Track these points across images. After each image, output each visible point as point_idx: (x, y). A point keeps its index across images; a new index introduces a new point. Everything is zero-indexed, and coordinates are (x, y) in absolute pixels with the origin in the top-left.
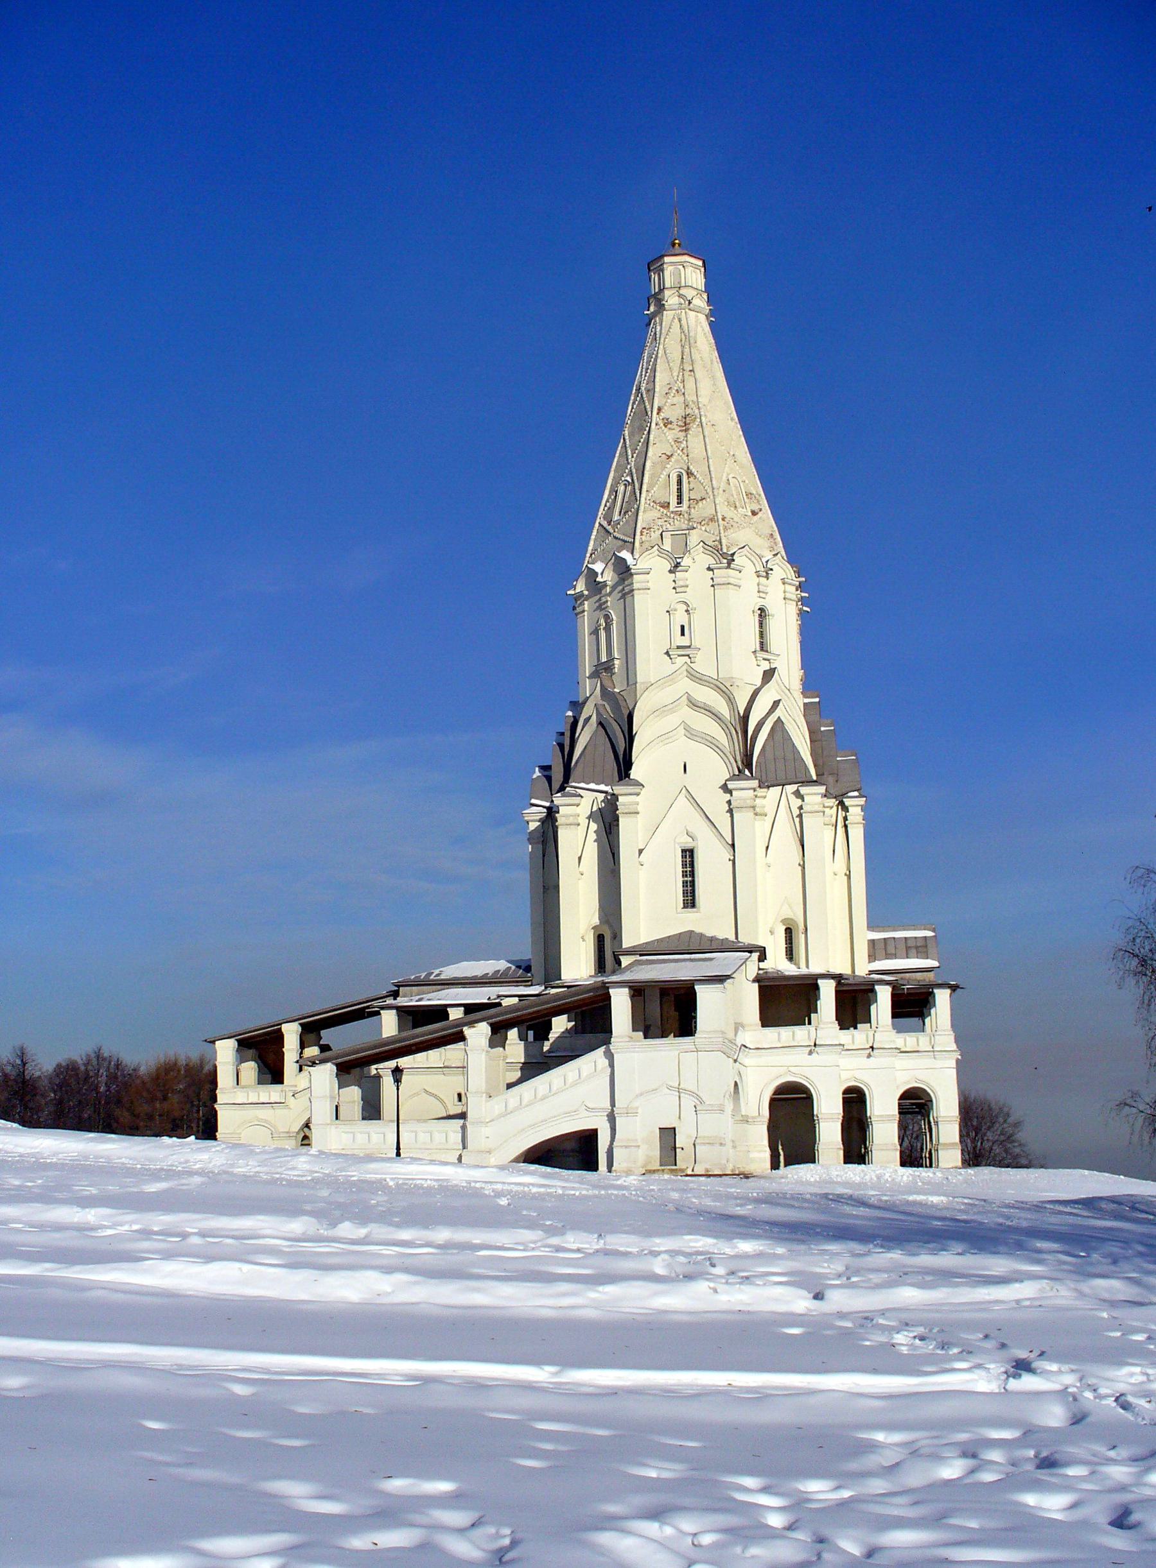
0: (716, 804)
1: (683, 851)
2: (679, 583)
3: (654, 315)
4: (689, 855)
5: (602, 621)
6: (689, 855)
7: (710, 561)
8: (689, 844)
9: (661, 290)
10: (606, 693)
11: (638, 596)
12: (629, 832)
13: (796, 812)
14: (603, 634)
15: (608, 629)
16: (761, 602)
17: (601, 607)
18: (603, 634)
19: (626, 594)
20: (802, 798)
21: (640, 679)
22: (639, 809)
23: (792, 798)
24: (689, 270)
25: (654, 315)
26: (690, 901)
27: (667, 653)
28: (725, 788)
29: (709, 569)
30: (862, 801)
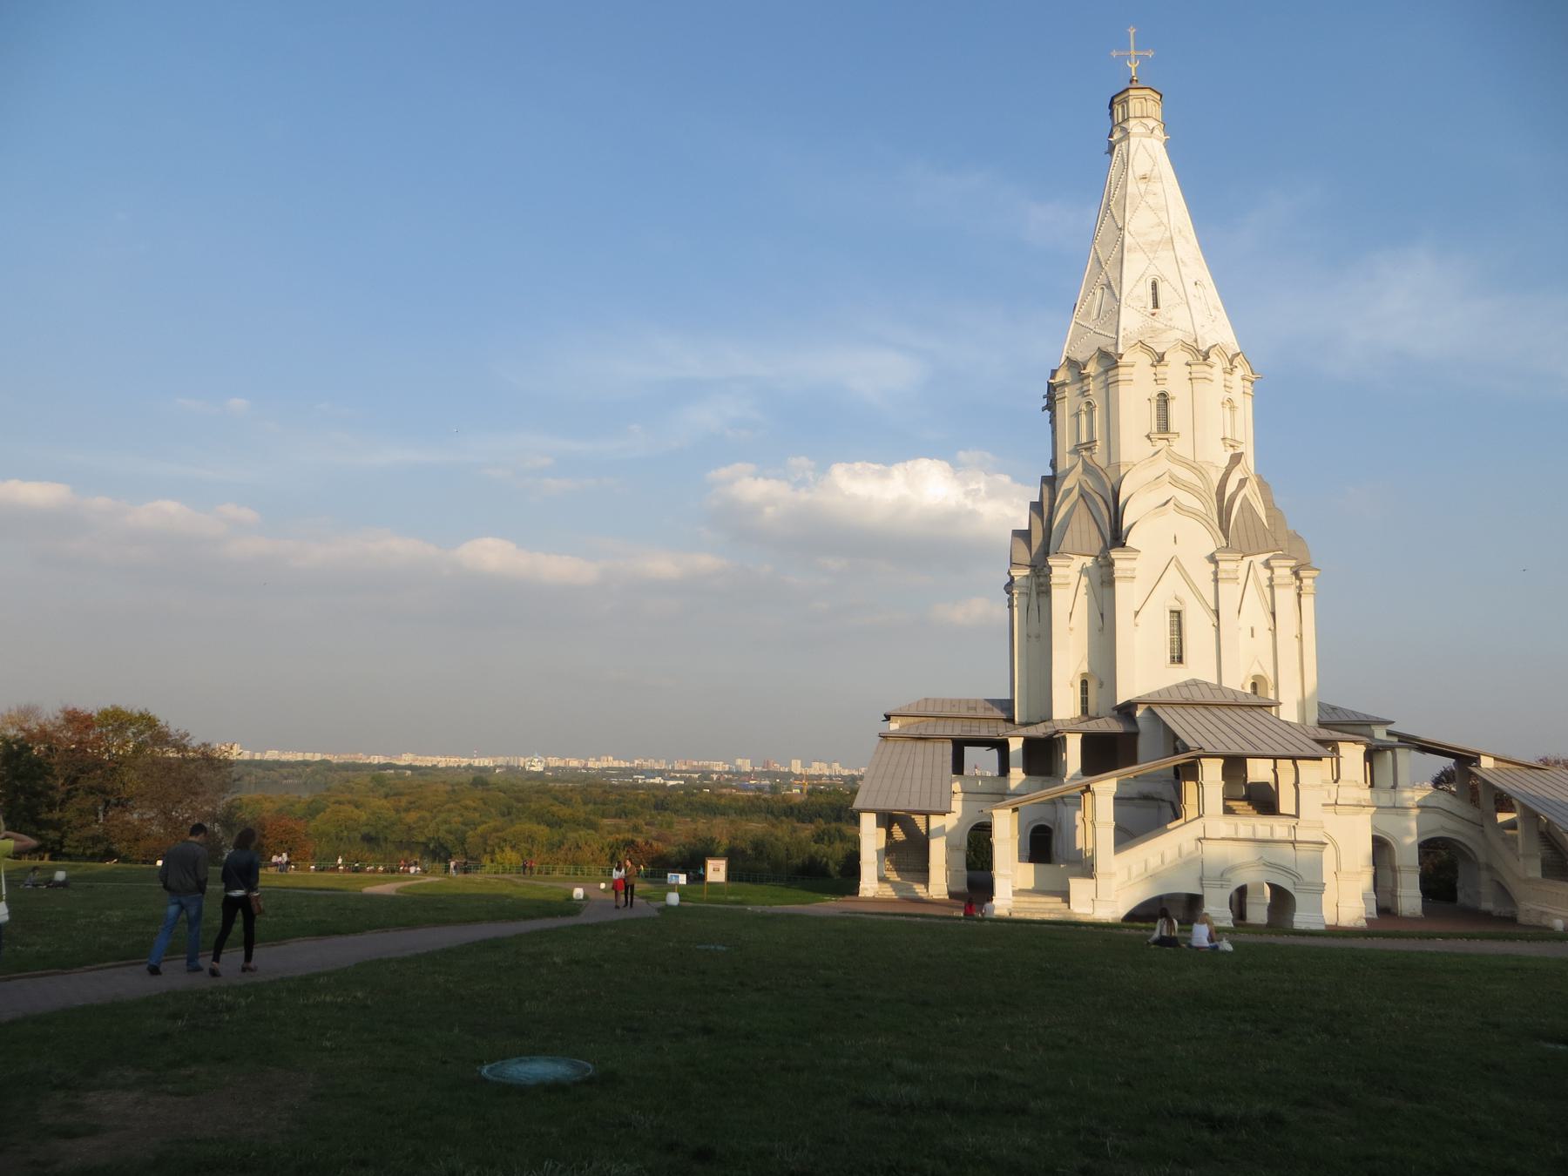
3: (1120, 140)
4: (1177, 615)
5: (1084, 407)
6: (1177, 615)
7: (1189, 358)
9: (1126, 120)
10: (1088, 469)
11: (1122, 388)
12: (1126, 595)
14: (1084, 418)
15: (1090, 413)
16: (1225, 395)
17: (1084, 393)
18: (1084, 418)
19: (1109, 385)
20: (1272, 569)
21: (1124, 458)
22: (1136, 573)
24: (1150, 103)
25: (1120, 140)
26: (1178, 659)
27: (1148, 437)
28: (1212, 559)
30: (1315, 573)
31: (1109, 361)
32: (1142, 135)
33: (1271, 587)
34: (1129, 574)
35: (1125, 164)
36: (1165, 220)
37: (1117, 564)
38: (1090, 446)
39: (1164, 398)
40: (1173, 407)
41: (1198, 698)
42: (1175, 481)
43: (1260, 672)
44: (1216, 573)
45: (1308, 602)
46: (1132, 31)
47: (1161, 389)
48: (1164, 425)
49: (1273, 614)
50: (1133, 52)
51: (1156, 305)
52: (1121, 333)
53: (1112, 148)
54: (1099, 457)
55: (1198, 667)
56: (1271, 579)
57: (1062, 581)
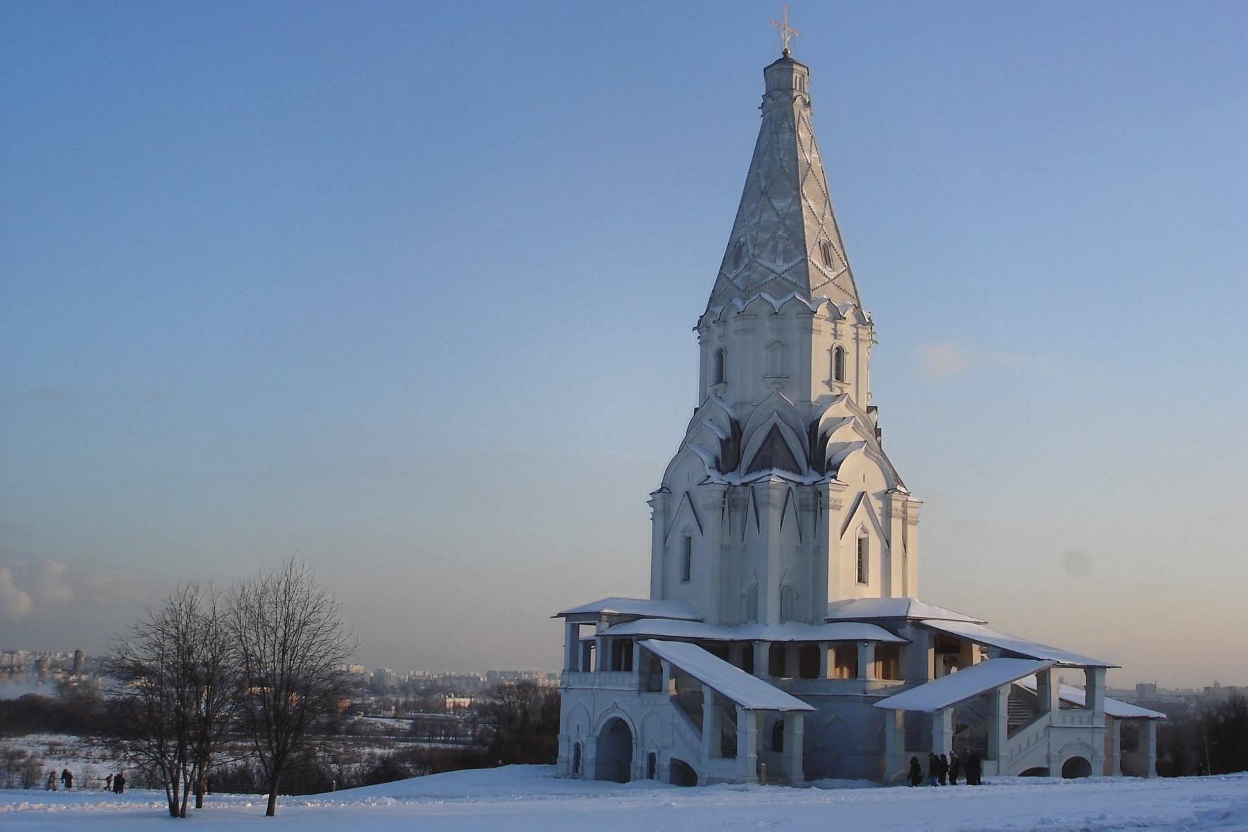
8: (864, 536)
12: (835, 519)
26: (861, 579)
39: (839, 353)
47: (838, 343)
55: (872, 590)
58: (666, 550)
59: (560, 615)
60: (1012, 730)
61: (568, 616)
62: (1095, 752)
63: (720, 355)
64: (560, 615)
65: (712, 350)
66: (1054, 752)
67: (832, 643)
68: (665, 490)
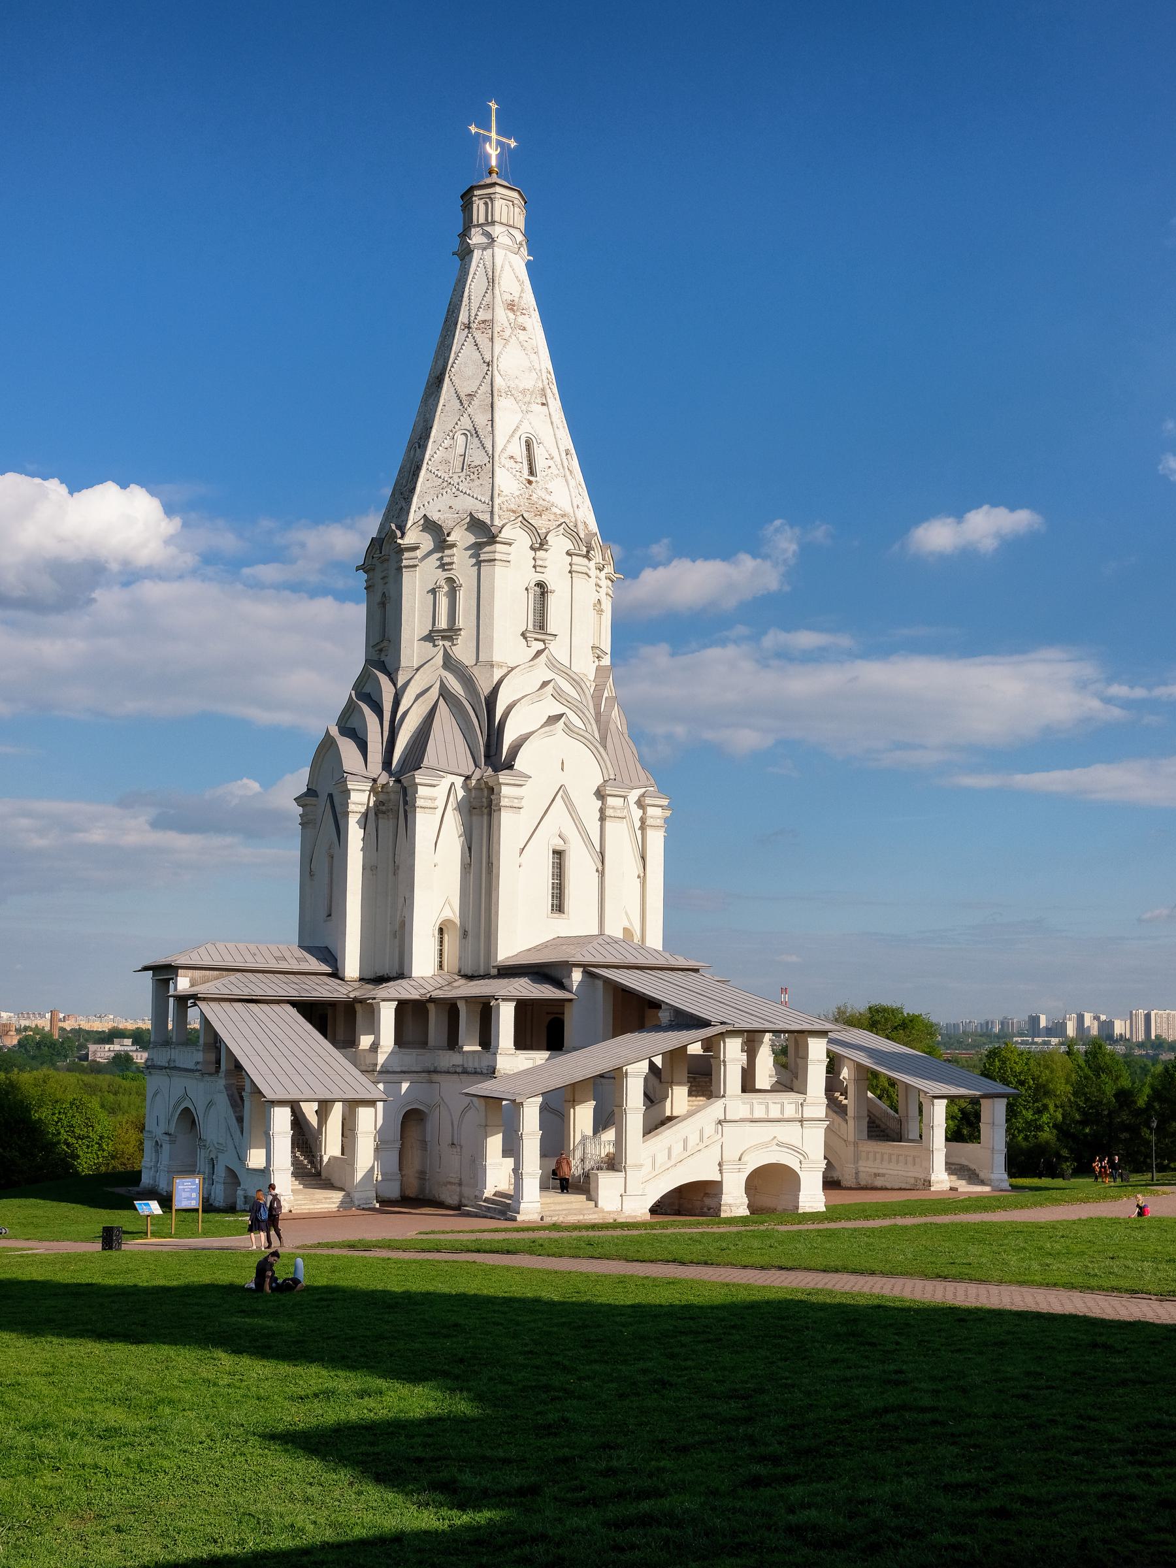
0: (589, 808)
1: (555, 852)
2: (539, 563)
4: (559, 854)
8: (559, 844)
12: (511, 827)
13: (638, 824)
22: (523, 803)
23: (633, 807)
26: (559, 906)
27: (523, 635)
29: (569, 554)
31: (484, 534)
32: (507, 248)
33: (643, 828)
34: (516, 803)
35: (492, 282)
36: (537, 366)
37: (505, 790)
38: (451, 633)
40: (552, 601)
41: (632, 960)
42: (559, 695)
43: (627, 925)
44: (602, 811)
45: (656, 841)
46: (494, 106)
47: (540, 577)
48: (541, 624)
49: (643, 858)
50: (494, 135)
51: (532, 472)
52: (497, 501)
53: (465, 253)
54: (463, 651)
55: (579, 921)
56: (643, 820)
57: (429, 804)
58: (311, 874)
59: (146, 969)
60: (656, 1122)
61: (155, 969)
62: (805, 1155)
63: (383, 604)
64: (146, 969)
65: (378, 598)
66: (731, 1155)
67: (468, 1000)
68: (311, 792)
